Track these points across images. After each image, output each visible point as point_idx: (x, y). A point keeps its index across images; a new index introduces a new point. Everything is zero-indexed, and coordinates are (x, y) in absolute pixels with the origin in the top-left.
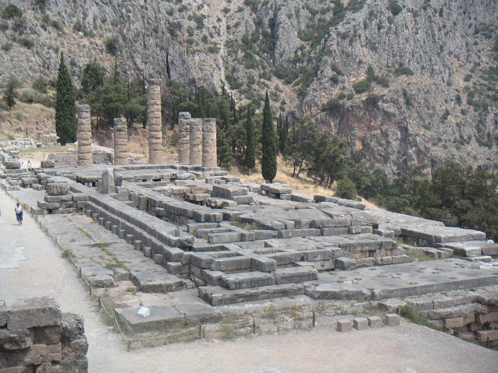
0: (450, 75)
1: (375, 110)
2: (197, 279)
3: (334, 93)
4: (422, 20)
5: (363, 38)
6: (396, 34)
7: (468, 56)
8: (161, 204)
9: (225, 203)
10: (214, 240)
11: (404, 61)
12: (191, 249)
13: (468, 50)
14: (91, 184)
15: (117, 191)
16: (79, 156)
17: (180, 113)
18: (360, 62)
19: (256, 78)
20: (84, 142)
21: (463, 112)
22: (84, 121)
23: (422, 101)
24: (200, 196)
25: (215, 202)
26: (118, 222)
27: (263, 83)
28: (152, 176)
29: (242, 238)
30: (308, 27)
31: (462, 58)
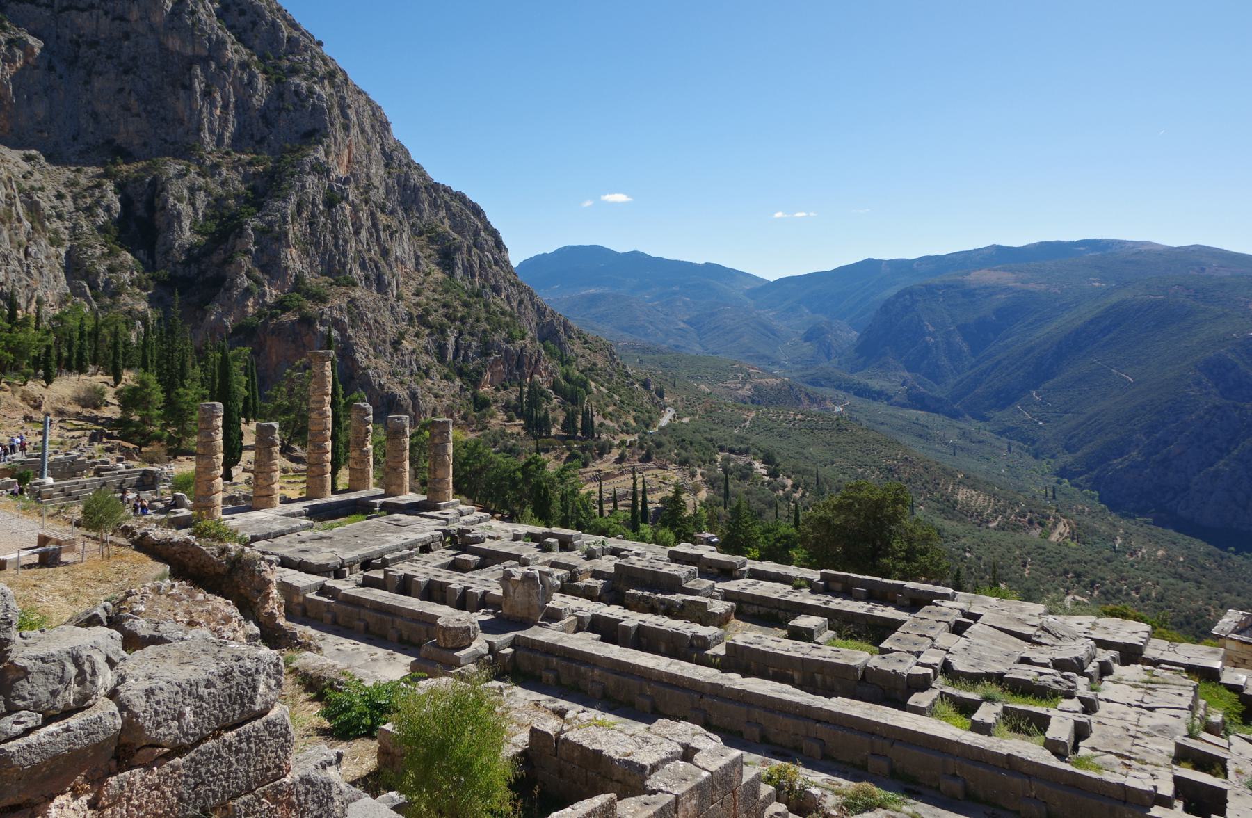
0: (398, 286)
4: (363, 216)
5: (290, 236)
6: (332, 232)
7: (417, 264)
9: (691, 601)
11: (344, 267)
13: (417, 258)
15: (554, 616)
18: (287, 268)
21: (417, 335)
23: (372, 322)
24: (598, 584)
25: (671, 603)
28: (418, 541)
30: (205, 216)
31: (410, 264)
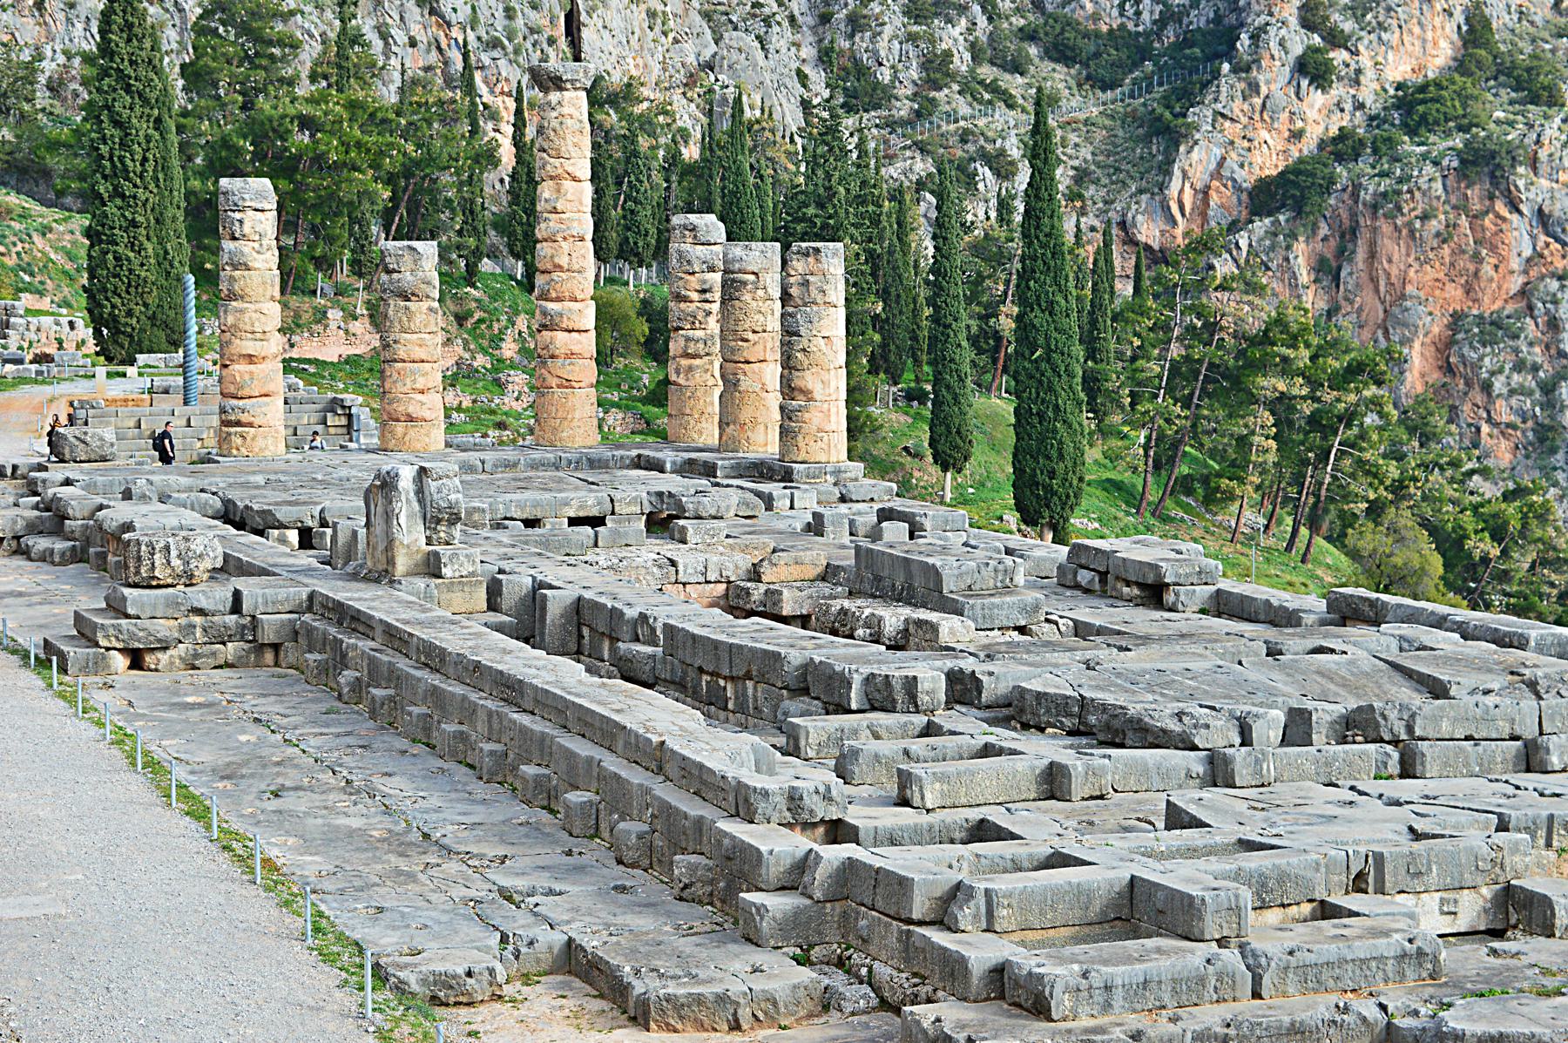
1: (1500, 207)
2: (883, 971)
3: (1314, 134)
8: (642, 627)
9: (920, 623)
10: (928, 796)
12: (838, 831)
14: (293, 536)
16: (223, 411)
17: (677, 220)
19: (961, 62)
20: (249, 347)
22: (246, 248)
26: (469, 712)
27: (993, 88)
29: (1053, 783)
